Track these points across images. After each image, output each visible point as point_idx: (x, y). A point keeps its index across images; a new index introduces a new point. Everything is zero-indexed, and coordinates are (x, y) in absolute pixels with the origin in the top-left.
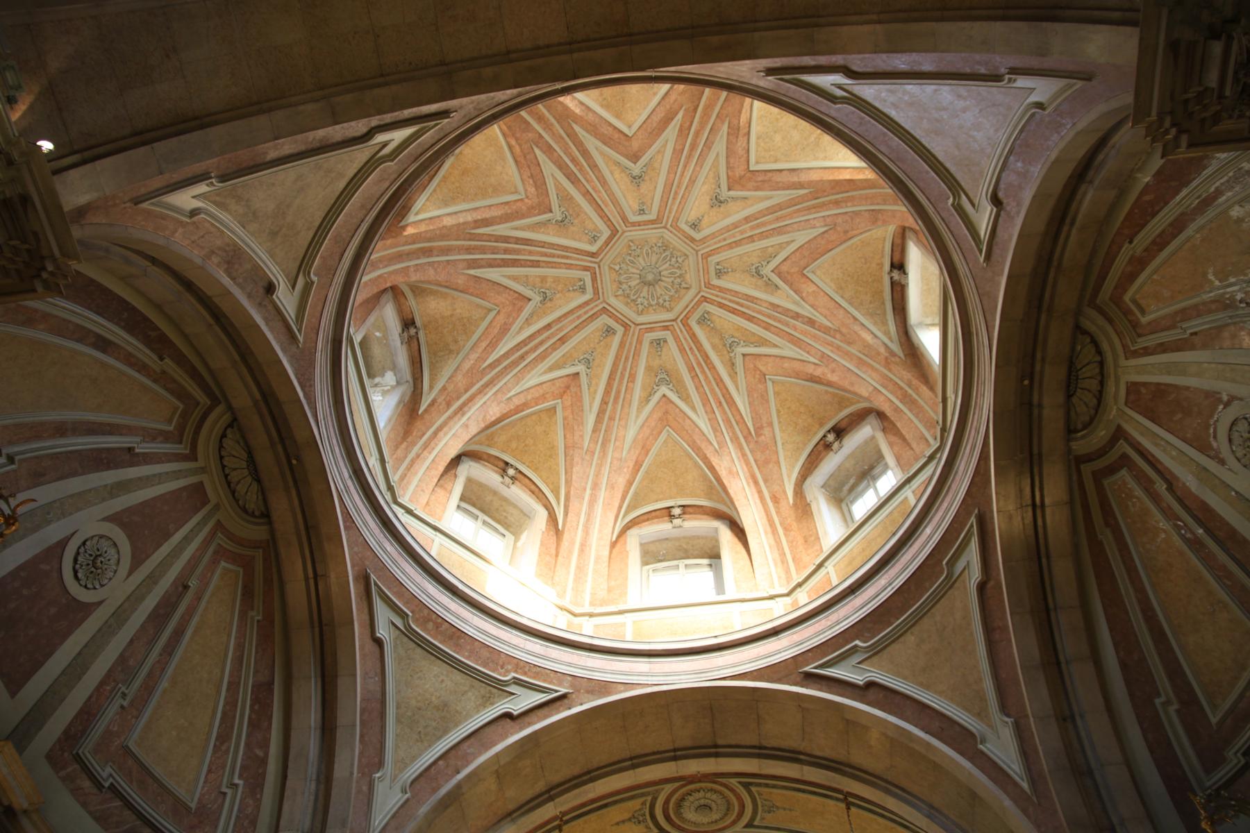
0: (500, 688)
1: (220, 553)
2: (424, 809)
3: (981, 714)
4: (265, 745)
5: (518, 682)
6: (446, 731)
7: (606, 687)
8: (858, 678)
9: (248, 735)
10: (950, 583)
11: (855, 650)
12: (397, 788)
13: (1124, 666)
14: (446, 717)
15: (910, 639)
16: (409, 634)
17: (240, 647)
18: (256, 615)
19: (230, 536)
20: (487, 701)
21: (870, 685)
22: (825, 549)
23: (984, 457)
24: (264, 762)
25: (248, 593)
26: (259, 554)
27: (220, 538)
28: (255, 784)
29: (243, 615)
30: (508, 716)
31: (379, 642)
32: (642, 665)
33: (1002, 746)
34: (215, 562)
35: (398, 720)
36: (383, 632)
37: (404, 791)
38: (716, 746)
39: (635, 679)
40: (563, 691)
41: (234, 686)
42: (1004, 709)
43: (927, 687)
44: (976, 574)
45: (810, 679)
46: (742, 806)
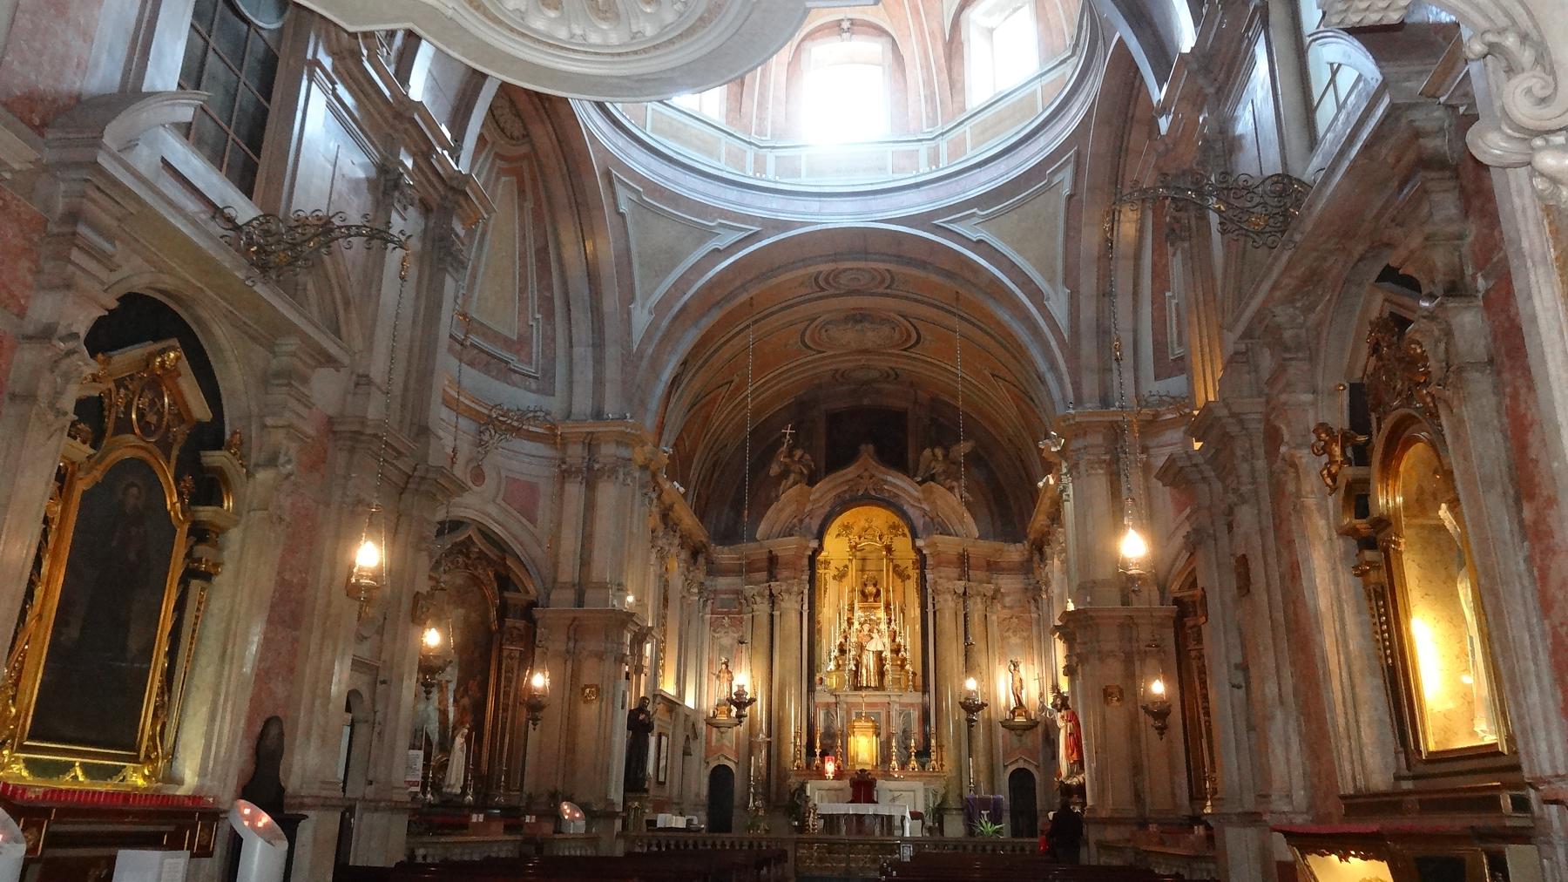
0: (708, 233)
1: (502, 172)
2: (665, 323)
3: (1051, 281)
4: (550, 287)
5: (721, 225)
6: (674, 266)
7: (787, 225)
8: (974, 236)
9: (539, 283)
10: (1049, 187)
11: (973, 215)
12: (646, 311)
13: (1154, 265)
14: (674, 258)
15: (1014, 216)
16: (642, 205)
17: (522, 228)
18: (529, 205)
19: (503, 158)
20: (701, 241)
21: (980, 241)
22: (968, 107)
23: (1088, 114)
24: (551, 299)
25: (522, 192)
26: (525, 164)
27: (499, 163)
28: (549, 315)
29: (521, 208)
30: (717, 250)
31: (622, 215)
32: (814, 205)
33: (1058, 306)
34: (497, 179)
35: (641, 265)
36: (623, 208)
37: (650, 313)
38: (867, 253)
39: (808, 218)
40: (756, 229)
41: (523, 256)
42: (1065, 283)
43: (1019, 252)
44: (1066, 191)
45: (938, 229)
46: (883, 281)
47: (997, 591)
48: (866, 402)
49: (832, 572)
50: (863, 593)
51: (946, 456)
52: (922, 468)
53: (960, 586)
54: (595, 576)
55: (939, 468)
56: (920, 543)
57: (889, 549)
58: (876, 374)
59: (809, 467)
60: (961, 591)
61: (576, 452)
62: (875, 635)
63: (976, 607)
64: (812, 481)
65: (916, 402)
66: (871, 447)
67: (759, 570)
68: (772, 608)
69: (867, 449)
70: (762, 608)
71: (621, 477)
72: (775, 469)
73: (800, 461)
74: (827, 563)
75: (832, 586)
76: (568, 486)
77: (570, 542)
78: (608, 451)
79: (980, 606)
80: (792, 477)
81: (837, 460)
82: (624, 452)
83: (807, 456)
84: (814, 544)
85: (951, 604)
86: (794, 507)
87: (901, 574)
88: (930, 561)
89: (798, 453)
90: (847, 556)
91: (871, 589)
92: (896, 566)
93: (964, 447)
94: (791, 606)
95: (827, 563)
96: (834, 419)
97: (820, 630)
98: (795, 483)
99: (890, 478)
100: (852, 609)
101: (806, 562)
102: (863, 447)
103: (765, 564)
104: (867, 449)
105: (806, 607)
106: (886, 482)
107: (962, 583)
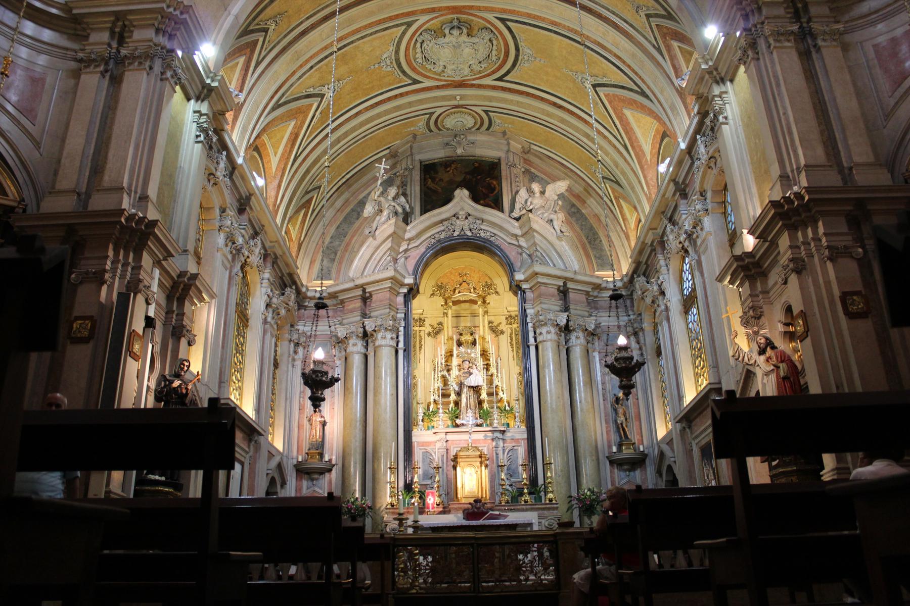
47: (598, 326)
48: (459, 151)
49: (427, 329)
50: (459, 344)
51: (543, 193)
52: (518, 206)
53: (562, 319)
54: (107, 179)
55: (537, 201)
56: (519, 276)
57: (484, 302)
58: (469, 122)
59: (404, 209)
60: (565, 322)
61: (100, 39)
62: (474, 371)
63: (577, 341)
64: (407, 218)
65: (508, 151)
66: (466, 192)
67: (352, 311)
68: (366, 347)
69: (462, 195)
70: (356, 347)
71: (158, 67)
72: (369, 210)
73: (394, 199)
74: (421, 321)
75: (428, 342)
76: (83, 77)
77: (78, 142)
78: (142, 36)
79: (582, 341)
80: (385, 213)
81: (434, 198)
82: (162, 40)
83: (402, 199)
84: (409, 280)
85: (555, 337)
86: (388, 244)
87: (495, 330)
88: (529, 295)
89: (392, 191)
90: (441, 310)
91: (467, 337)
92: (490, 322)
93: (561, 186)
94: (384, 340)
95: (421, 321)
96: (429, 170)
97: (415, 385)
98: (389, 219)
99: (485, 217)
100: (449, 355)
101: (400, 299)
102: (457, 192)
103: (358, 304)
104: (462, 195)
105: (401, 345)
106: (483, 220)
107: (565, 315)
